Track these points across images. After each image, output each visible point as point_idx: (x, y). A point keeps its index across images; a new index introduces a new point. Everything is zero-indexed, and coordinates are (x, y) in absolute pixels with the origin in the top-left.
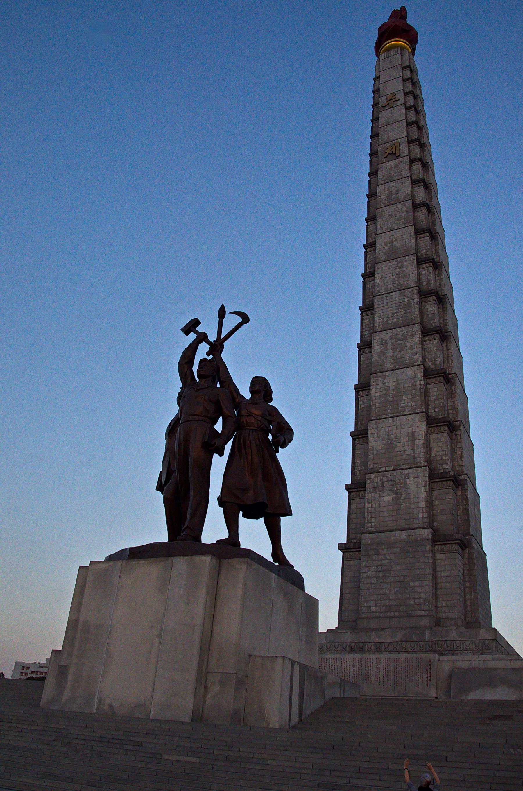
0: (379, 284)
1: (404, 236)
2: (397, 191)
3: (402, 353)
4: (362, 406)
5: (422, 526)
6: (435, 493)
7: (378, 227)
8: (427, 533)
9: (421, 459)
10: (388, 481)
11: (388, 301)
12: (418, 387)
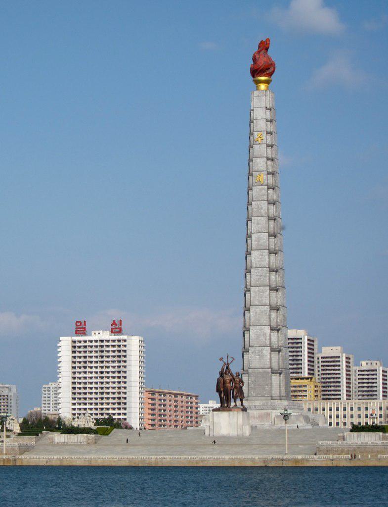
8: (269, 370)
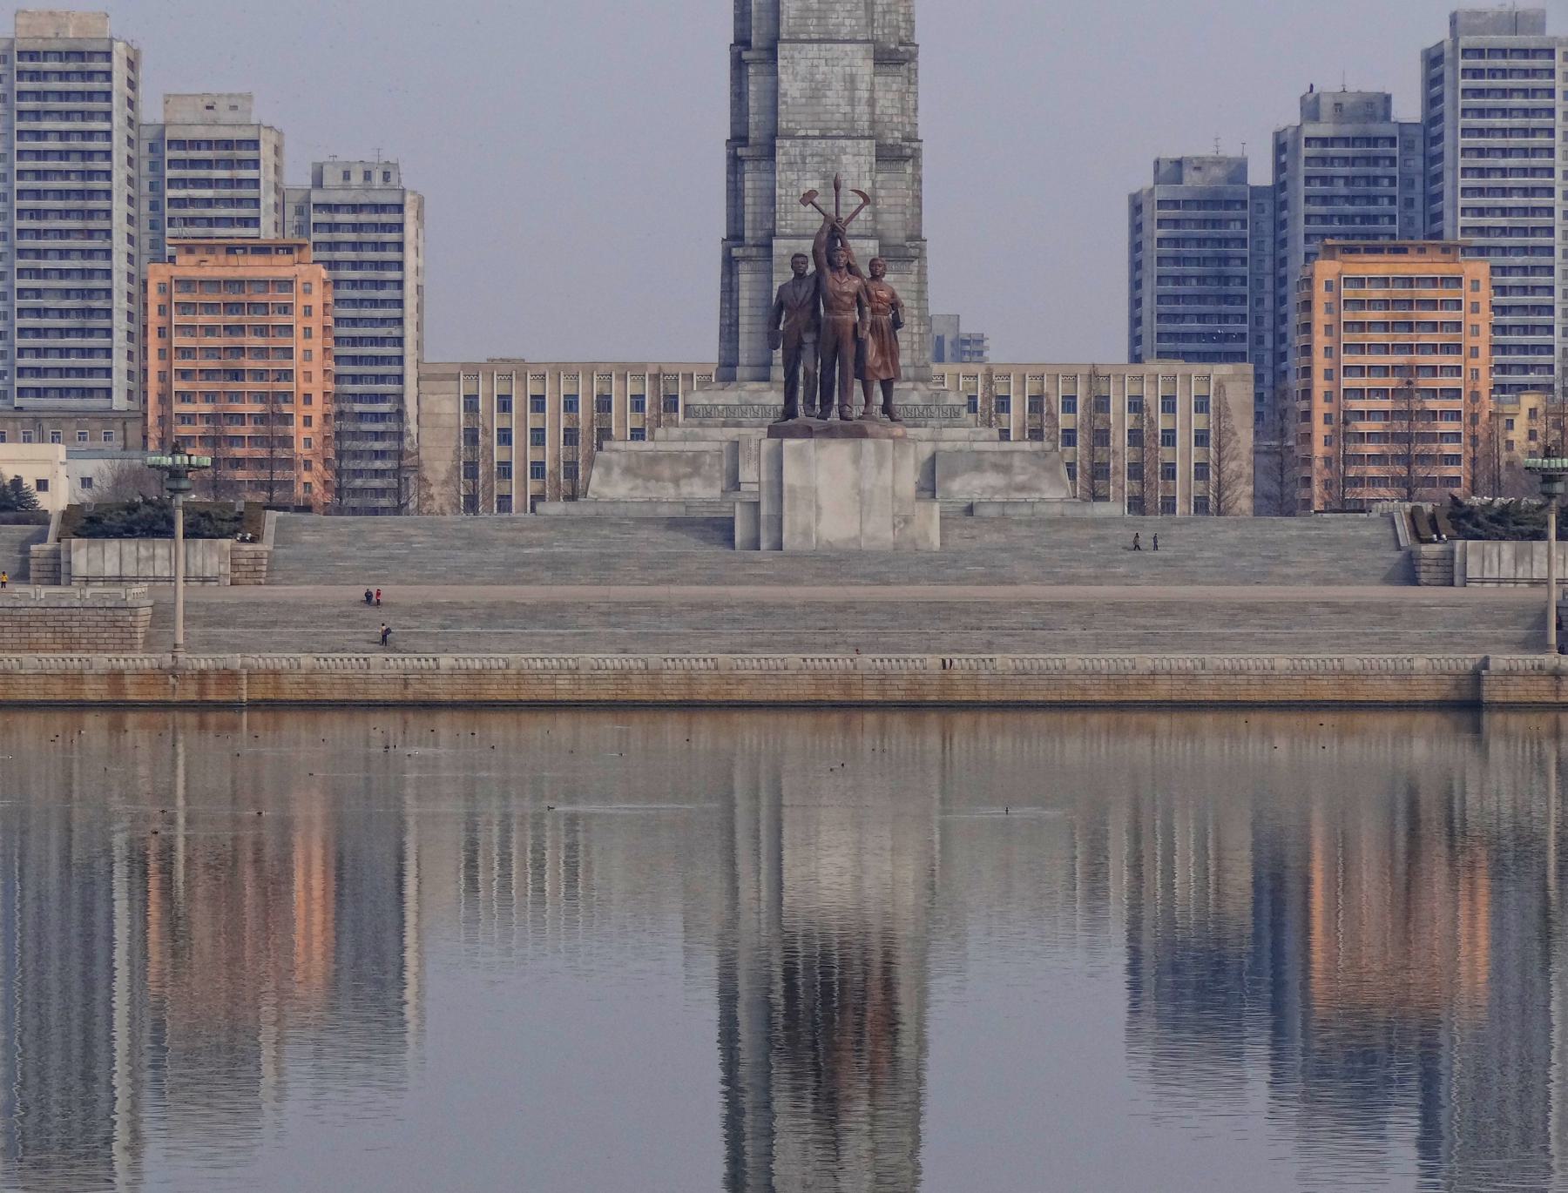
5: (863, 232)
9: (863, 125)
10: (812, 155)
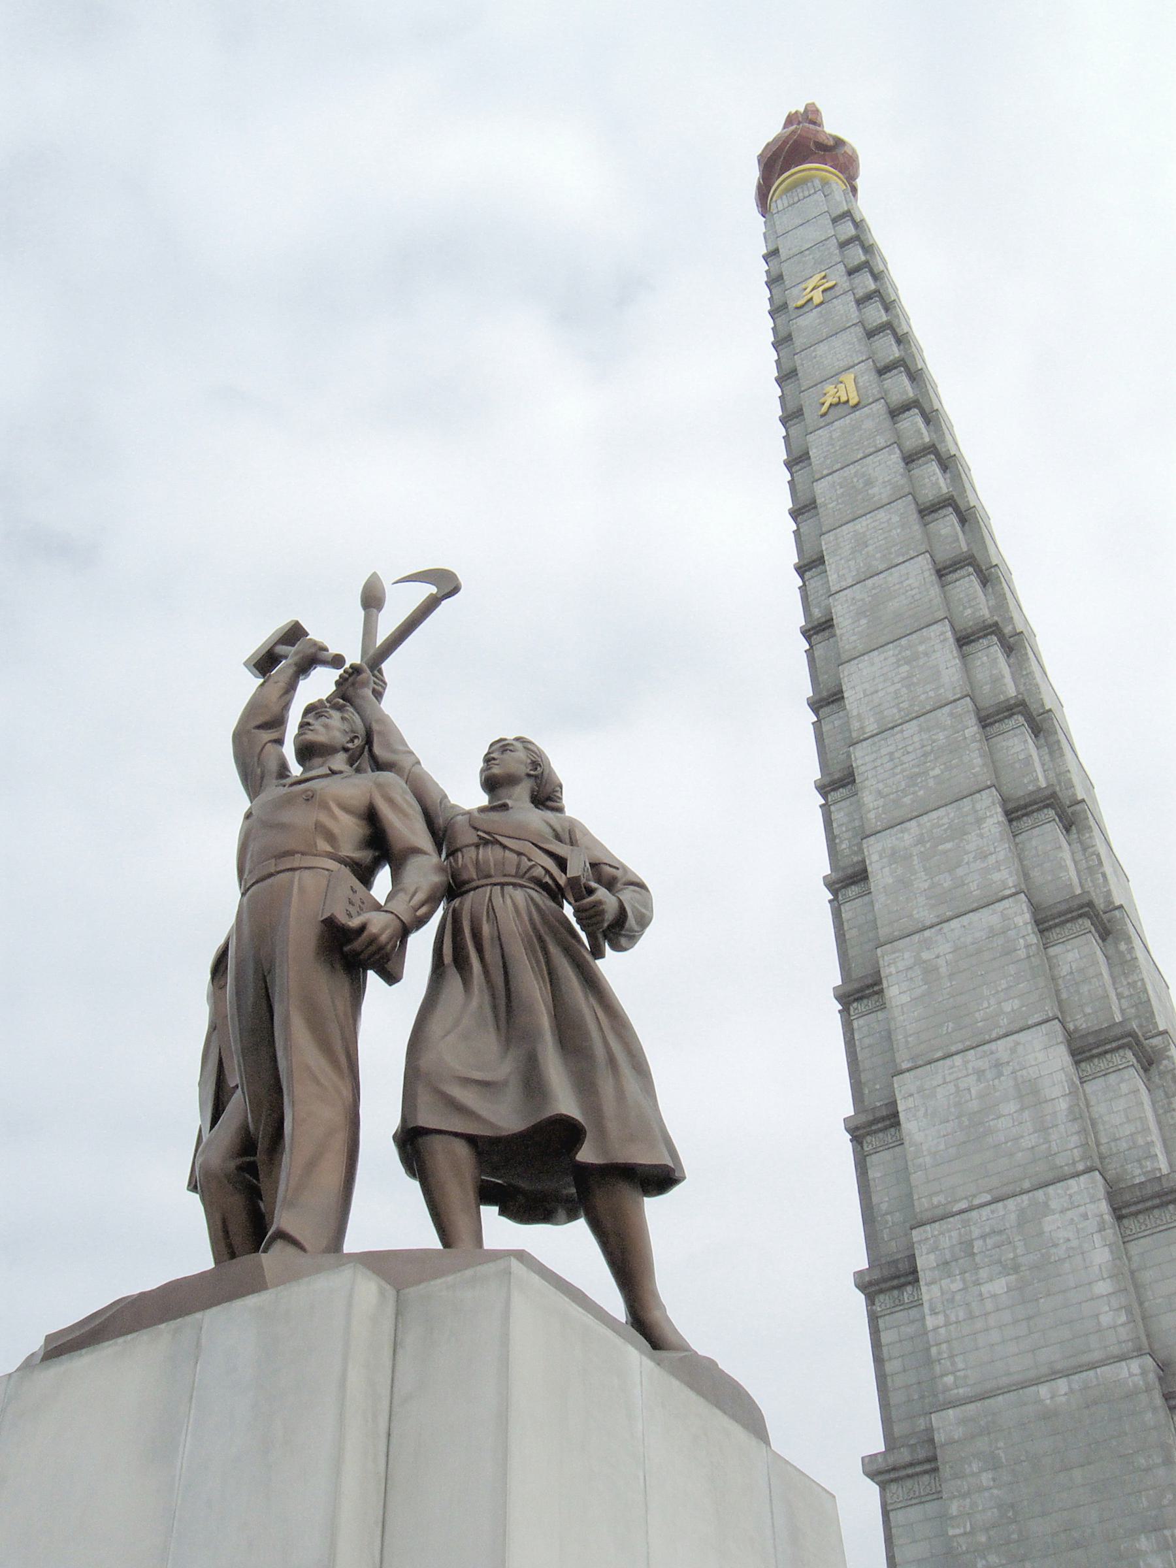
0: (859, 714)
1: (905, 584)
2: (869, 483)
3: (960, 872)
4: (867, 1041)
5: (1115, 1350)
6: (1134, 1249)
7: (832, 577)
10: (983, 1237)
11: (892, 748)
12: (1022, 953)
